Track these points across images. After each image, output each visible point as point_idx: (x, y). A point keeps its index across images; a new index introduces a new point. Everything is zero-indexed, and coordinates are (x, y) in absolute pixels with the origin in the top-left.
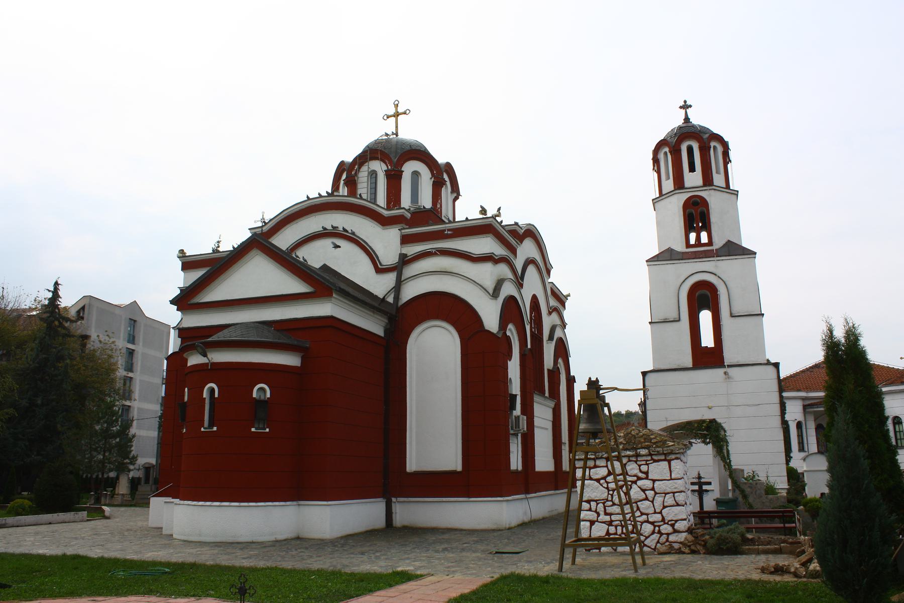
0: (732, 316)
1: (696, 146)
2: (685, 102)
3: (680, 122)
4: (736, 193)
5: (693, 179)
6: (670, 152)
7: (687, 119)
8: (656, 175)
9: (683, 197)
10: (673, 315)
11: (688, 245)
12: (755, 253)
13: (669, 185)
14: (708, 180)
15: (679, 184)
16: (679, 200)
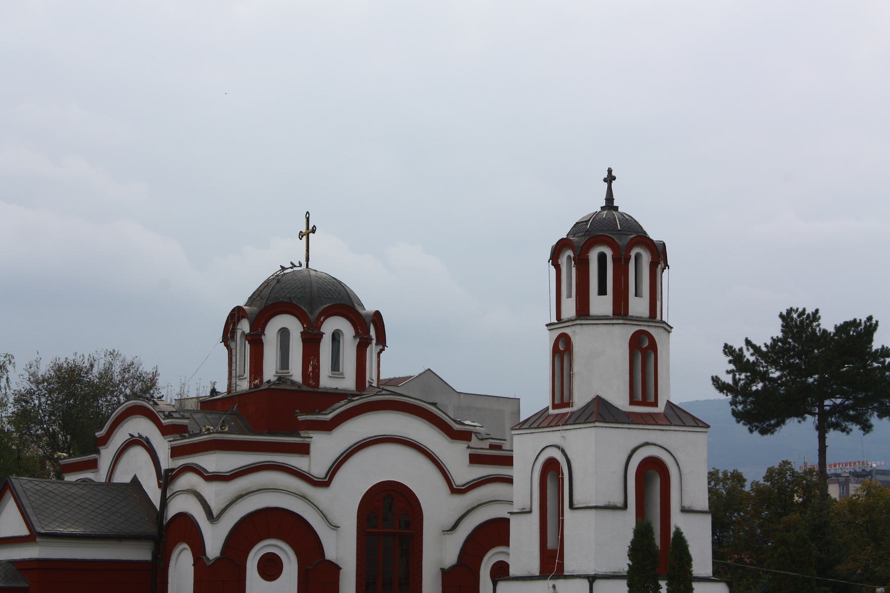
0: (684, 510)
1: (646, 258)
2: (610, 171)
4: (668, 329)
5: (638, 306)
6: (614, 259)
7: (610, 198)
8: (553, 270)
9: (631, 330)
10: (618, 500)
11: (633, 402)
12: (708, 427)
13: (601, 305)
16: (622, 334)
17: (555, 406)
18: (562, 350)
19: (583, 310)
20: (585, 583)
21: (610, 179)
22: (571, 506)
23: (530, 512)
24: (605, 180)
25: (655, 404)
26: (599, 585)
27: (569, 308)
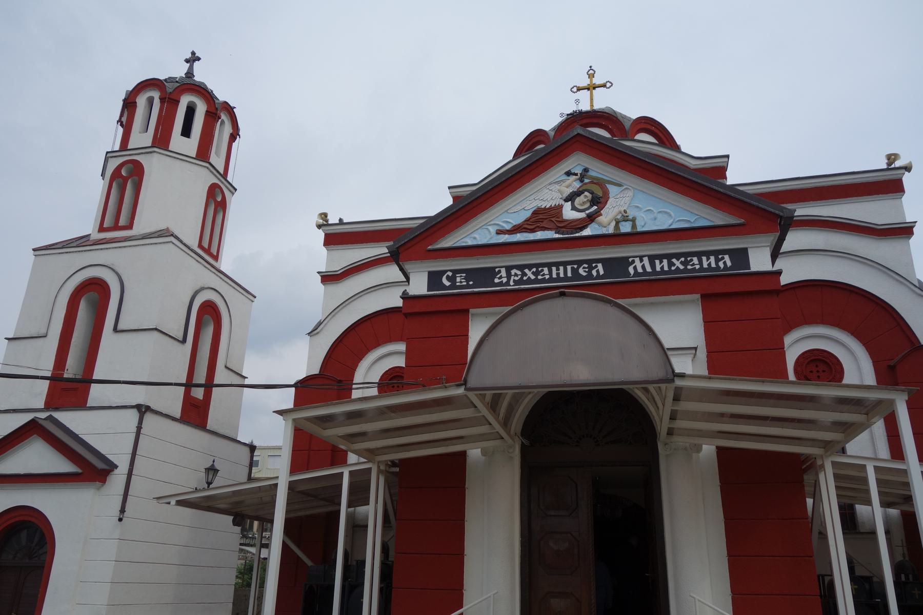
2: (193, 53)
3: (179, 71)
5: (217, 160)
7: (190, 74)
11: (200, 246)
14: (225, 175)
15: (203, 153)
16: (202, 179)
17: (102, 229)
18: (125, 177)
19: (161, 141)
20: (133, 415)
21: (193, 59)
22: (115, 330)
24: (187, 61)
25: (216, 258)
26: (149, 418)
27: (141, 138)
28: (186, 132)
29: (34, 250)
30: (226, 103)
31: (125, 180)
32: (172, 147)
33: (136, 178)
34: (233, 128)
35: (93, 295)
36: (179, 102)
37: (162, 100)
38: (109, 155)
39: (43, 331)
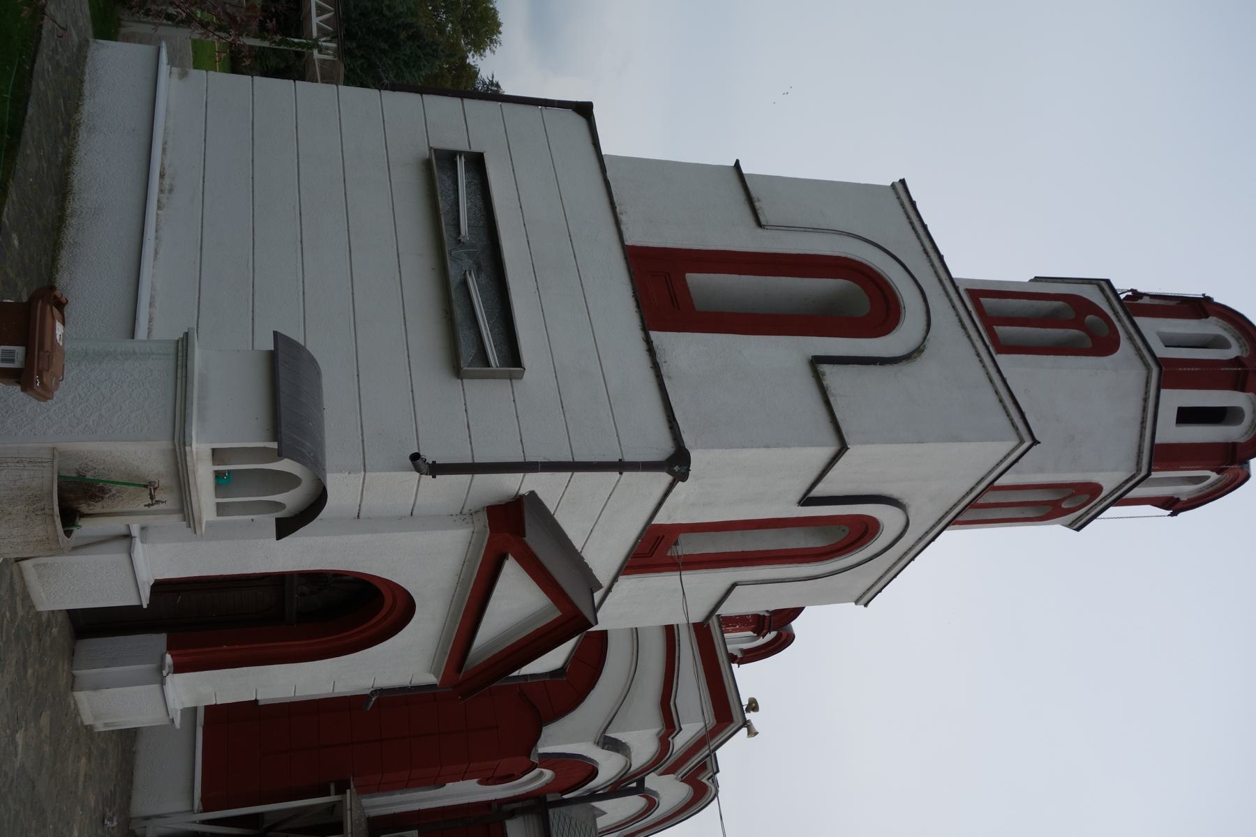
19: (1173, 374)
22: (816, 362)
23: (759, 225)
28: (1187, 416)
29: (903, 182)
30: (1247, 477)
31: (1078, 323)
32: (1164, 392)
33: (1089, 344)
34: (1190, 501)
35: (863, 305)
36: (1243, 390)
37: (1237, 361)
38: (1103, 284)
39: (763, 221)
